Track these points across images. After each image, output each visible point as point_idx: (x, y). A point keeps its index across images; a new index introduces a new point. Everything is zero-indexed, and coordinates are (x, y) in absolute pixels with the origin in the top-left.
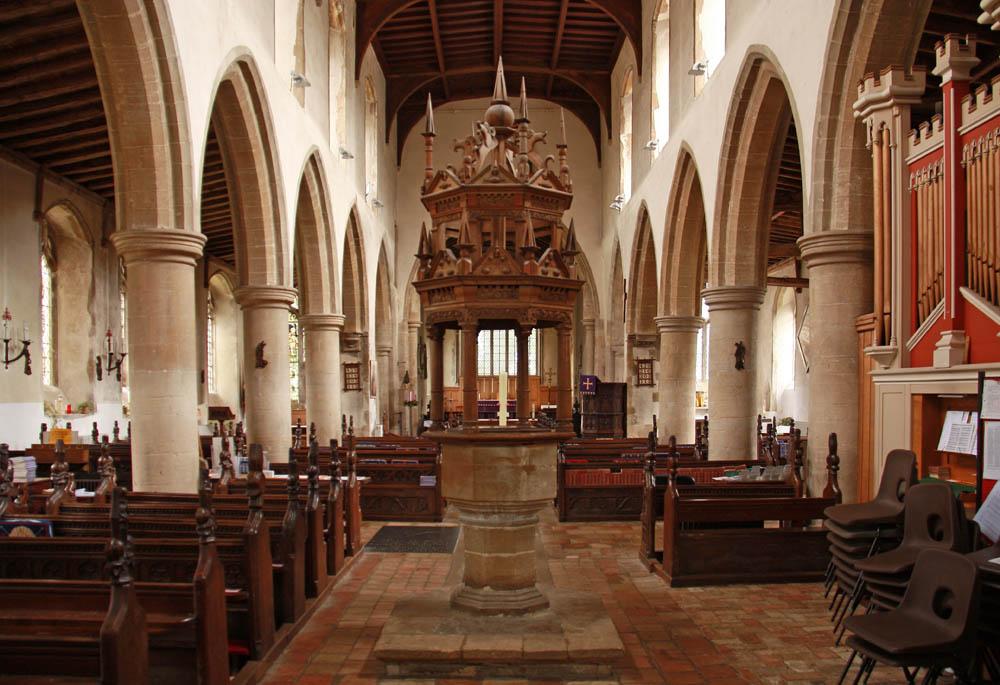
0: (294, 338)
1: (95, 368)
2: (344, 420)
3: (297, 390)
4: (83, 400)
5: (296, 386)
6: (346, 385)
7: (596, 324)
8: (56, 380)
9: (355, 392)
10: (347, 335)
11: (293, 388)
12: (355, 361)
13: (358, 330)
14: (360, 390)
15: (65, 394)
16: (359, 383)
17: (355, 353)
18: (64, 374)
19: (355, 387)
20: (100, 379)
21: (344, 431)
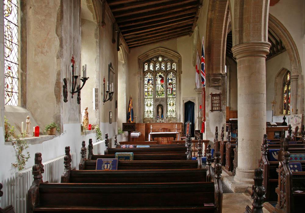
0: (151, 85)
1: (62, 89)
2: (217, 130)
3: (152, 112)
4: (50, 122)
5: (152, 111)
6: (212, 107)
7: (299, 77)
8: (24, 103)
9: (218, 112)
10: (215, 75)
11: (151, 112)
12: (218, 92)
13: (221, 72)
14: (221, 110)
15: (33, 115)
16: (220, 107)
17: (217, 87)
18: (32, 96)
19: (217, 108)
20: (66, 101)
21: (217, 137)
